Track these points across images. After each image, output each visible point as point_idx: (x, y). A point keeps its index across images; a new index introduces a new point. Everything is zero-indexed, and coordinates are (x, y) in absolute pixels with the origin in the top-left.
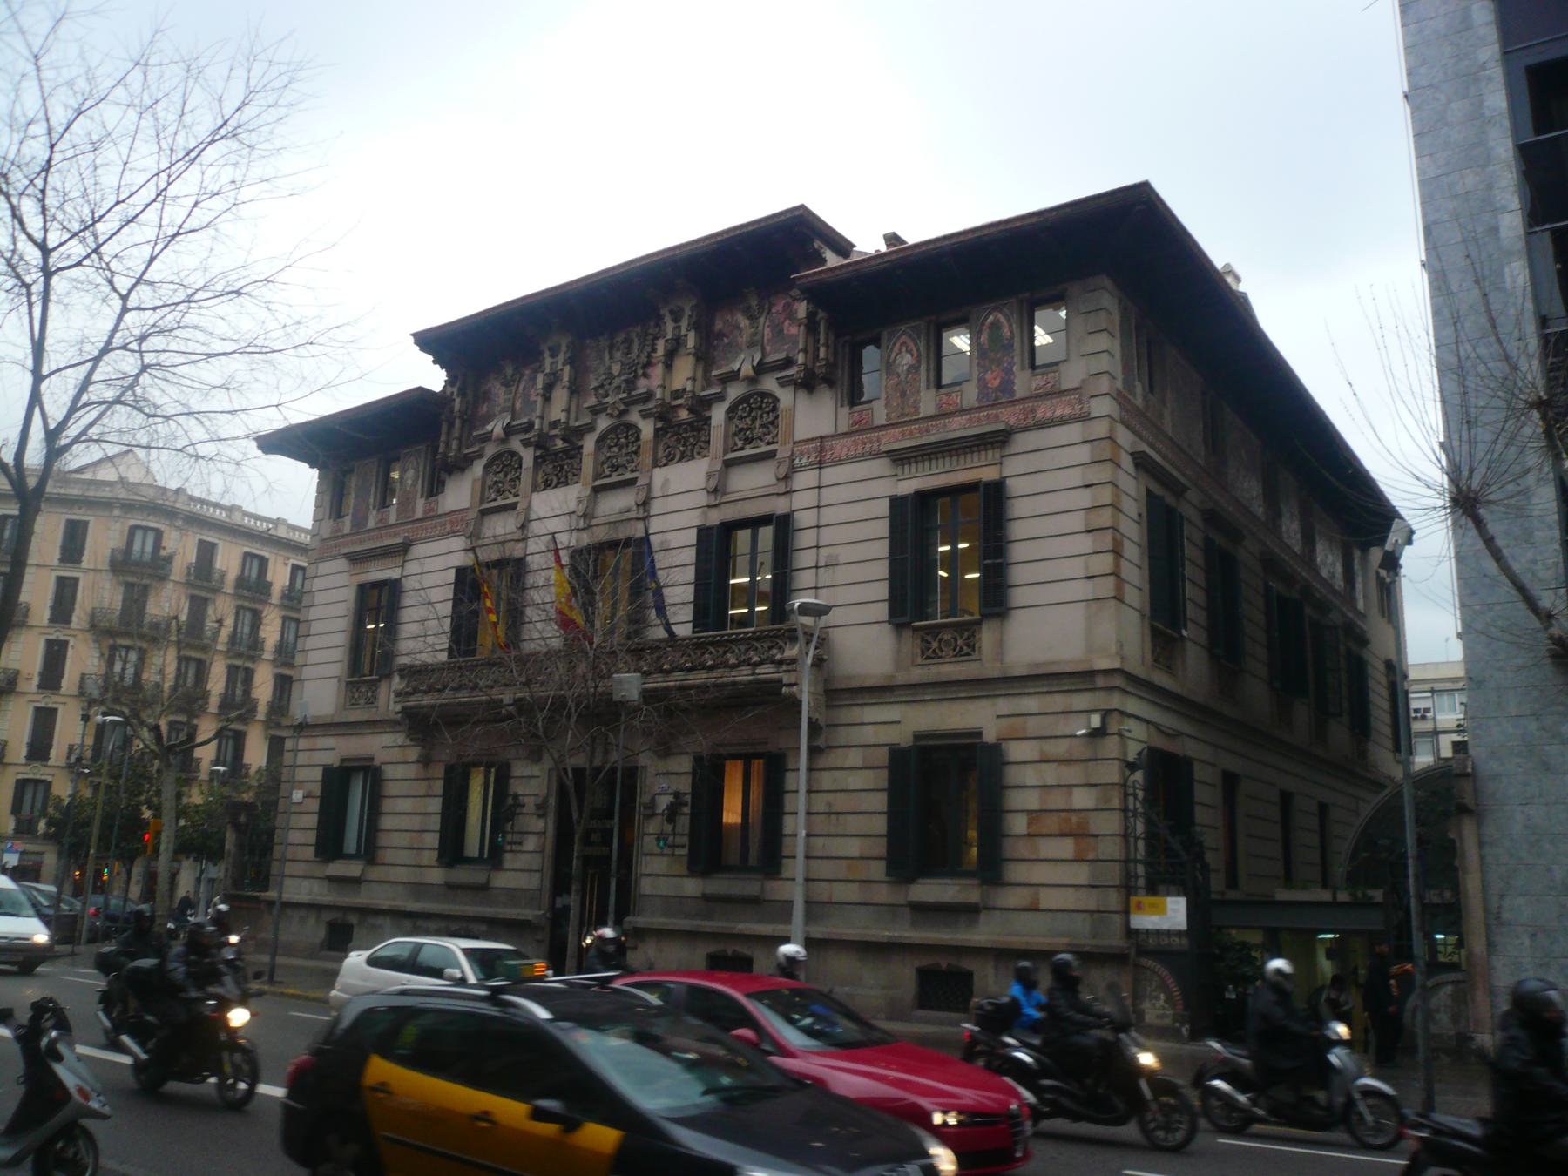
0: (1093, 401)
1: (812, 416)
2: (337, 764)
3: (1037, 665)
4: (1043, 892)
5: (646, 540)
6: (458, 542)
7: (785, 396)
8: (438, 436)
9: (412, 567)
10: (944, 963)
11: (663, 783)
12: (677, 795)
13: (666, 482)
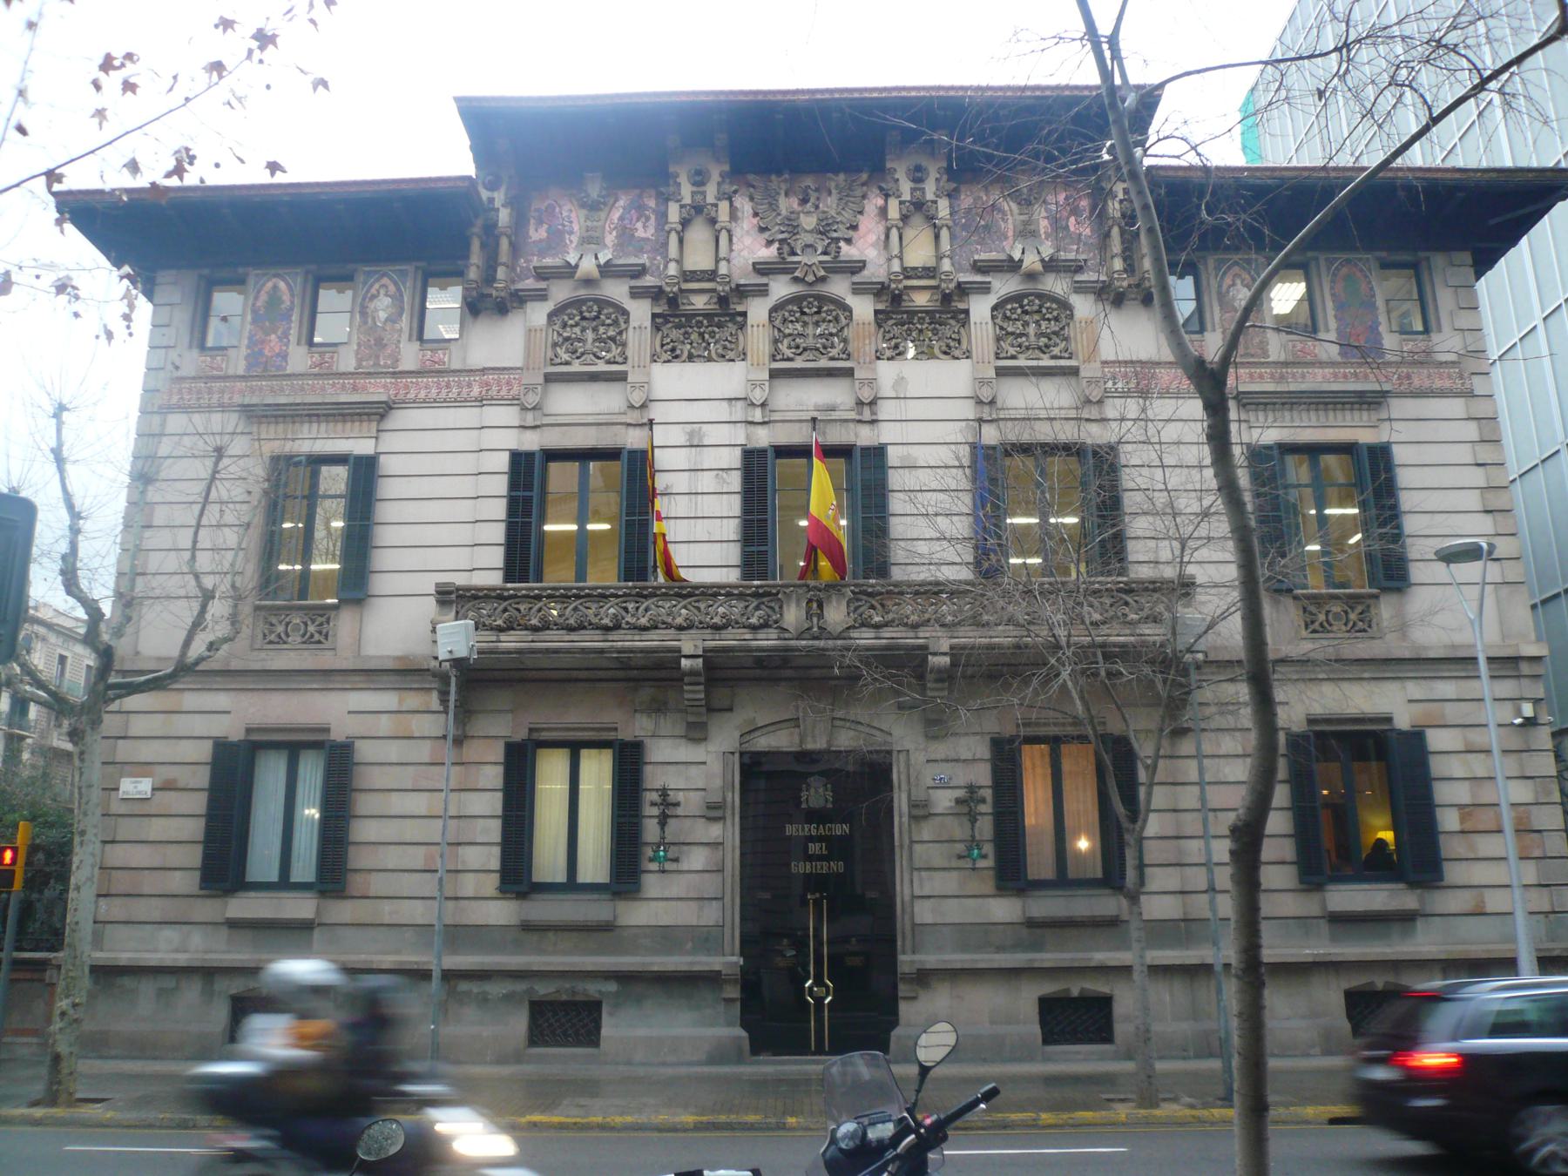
0: (1476, 379)
1: (1131, 337)
2: (236, 735)
3: (1454, 647)
4: (1488, 893)
5: (877, 454)
6: (509, 415)
7: (1083, 307)
8: (467, 257)
9: (390, 442)
10: (1380, 981)
11: (943, 771)
12: (972, 789)
13: (900, 381)
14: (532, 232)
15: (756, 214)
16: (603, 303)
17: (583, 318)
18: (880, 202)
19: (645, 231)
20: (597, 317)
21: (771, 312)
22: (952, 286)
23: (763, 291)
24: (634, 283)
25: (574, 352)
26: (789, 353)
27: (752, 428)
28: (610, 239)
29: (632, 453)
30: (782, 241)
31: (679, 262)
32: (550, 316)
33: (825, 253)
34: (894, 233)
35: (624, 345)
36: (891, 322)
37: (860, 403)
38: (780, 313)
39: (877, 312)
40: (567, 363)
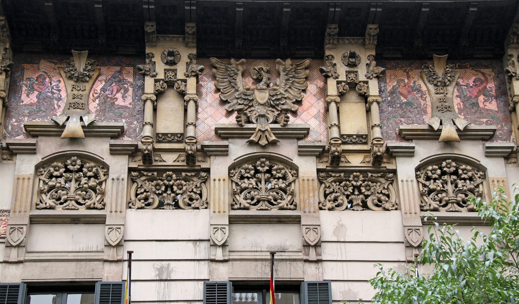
7: (495, 168)
13: (340, 227)
14: (23, 97)
15: (218, 90)
16: (85, 158)
17: (67, 171)
18: (321, 84)
19: (124, 100)
20: (80, 170)
21: (230, 169)
22: (383, 149)
23: (224, 152)
24: (113, 142)
25: (59, 199)
26: (245, 203)
27: (214, 265)
28: (93, 106)
29: (105, 286)
30: (240, 111)
31: (153, 125)
32: (37, 167)
33: (275, 122)
34: (333, 107)
35: (103, 193)
36: (330, 179)
37: (307, 246)
38: (238, 170)
39: (319, 171)
40: (51, 208)
